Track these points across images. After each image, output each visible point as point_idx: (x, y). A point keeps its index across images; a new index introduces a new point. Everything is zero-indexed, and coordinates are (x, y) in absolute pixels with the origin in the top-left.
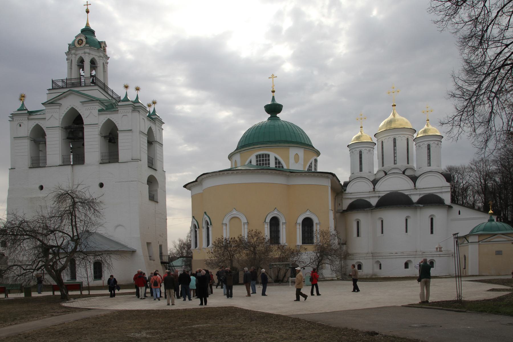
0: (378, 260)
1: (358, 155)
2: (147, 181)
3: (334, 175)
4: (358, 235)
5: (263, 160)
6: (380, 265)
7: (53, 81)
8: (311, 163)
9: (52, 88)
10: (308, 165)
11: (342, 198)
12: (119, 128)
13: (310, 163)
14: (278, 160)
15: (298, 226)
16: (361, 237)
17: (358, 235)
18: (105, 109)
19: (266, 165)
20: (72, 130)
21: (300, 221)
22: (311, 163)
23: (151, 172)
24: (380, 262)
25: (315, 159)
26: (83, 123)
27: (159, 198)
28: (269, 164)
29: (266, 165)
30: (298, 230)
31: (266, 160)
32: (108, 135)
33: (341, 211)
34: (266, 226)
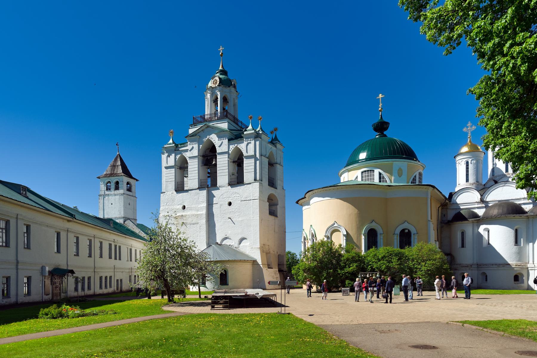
0: (484, 271)
1: (465, 166)
2: (268, 199)
3: (433, 187)
4: (463, 246)
5: (368, 176)
6: (486, 276)
7: (193, 117)
8: (415, 176)
9: (193, 124)
10: (412, 179)
11: (447, 209)
12: (245, 154)
13: (414, 176)
14: (382, 175)
15: (395, 237)
16: (465, 247)
17: (463, 246)
18: (234, 138)
19: (371, 180)
20: (208, 158)
21: (398, 231)
22: (415, 176)
23: (271, 191)
24: (486, 274)
25: (419, 173)
26: (216, 151)
27: (279, 212)
28: (373, 179)
29: (371, 180)
30: (395, 241)
31: (371, 175)
32: (236, 160)
33: (446, 221)
34: (395, 237)
